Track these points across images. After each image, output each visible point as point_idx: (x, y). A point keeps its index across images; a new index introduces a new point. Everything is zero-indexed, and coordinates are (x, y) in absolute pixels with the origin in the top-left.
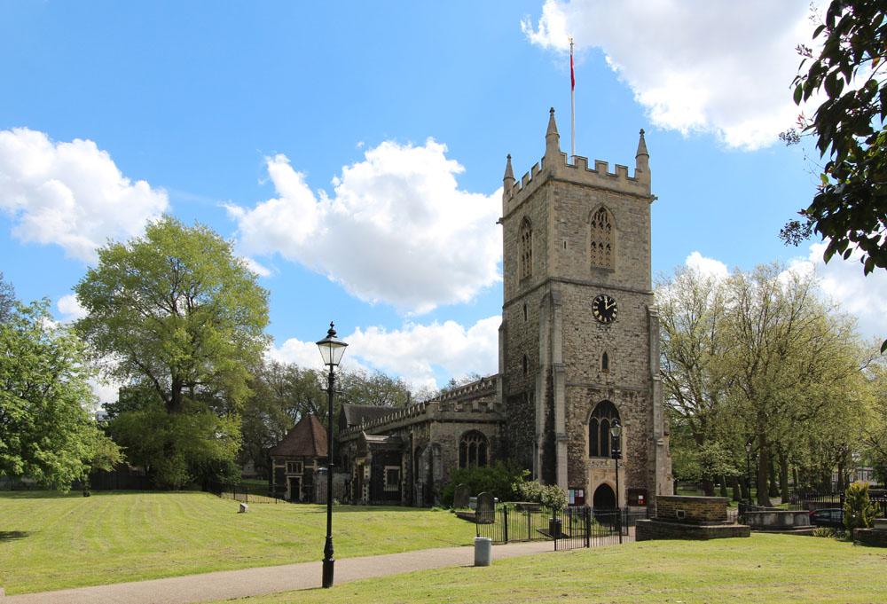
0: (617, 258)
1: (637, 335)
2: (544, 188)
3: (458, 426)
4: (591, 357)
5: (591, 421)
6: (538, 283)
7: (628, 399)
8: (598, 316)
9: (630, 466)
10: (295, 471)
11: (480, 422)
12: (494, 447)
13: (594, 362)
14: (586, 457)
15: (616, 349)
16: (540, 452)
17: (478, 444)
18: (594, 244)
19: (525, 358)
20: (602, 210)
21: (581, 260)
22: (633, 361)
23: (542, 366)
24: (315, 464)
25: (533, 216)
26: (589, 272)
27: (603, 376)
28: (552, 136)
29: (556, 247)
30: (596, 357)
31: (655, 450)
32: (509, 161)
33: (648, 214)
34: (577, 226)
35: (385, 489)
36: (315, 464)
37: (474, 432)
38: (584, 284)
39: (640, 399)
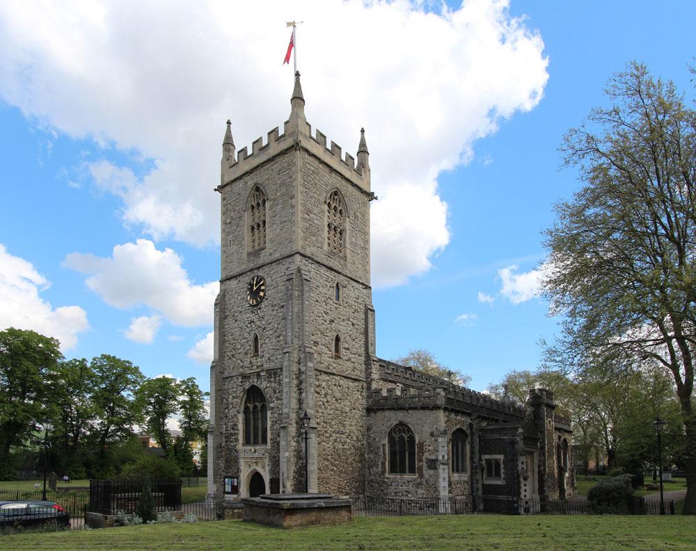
5: (245, 409)
14: (240, 446)
18: (253, 228)
27: (254, 360)
28: (298, 99)
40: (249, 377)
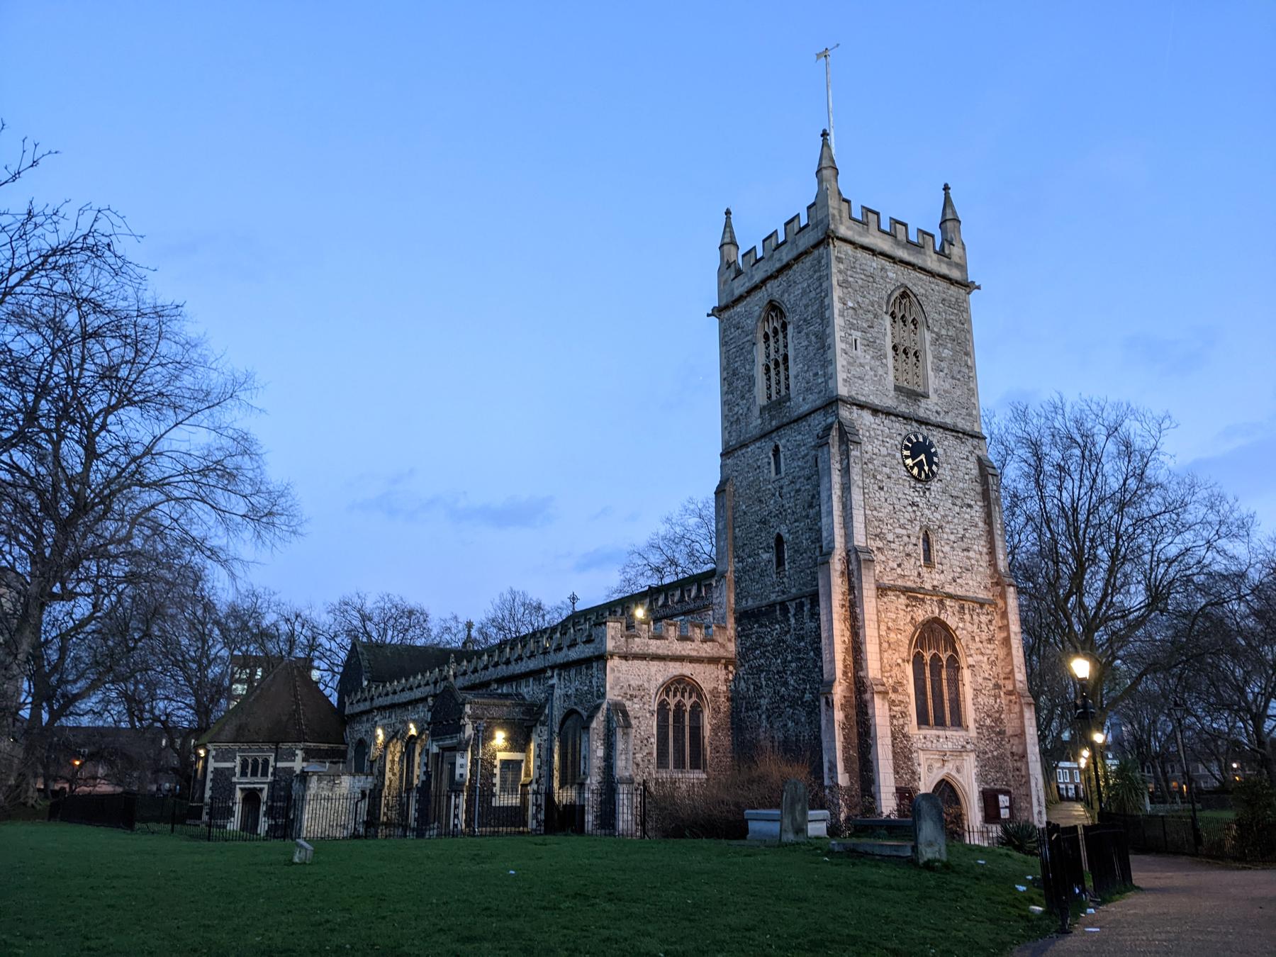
0: (931, 373)
1: (970, 506)
2: (816, 252)
3: (655, 666)
4: (906, 539)
6: (805, 408)
7: (967, 617)
8: (912, 468)
10: (254, 774)
11: (692, 660)
12: (716, 711)
13: (911, 546)
15: (940, 527)
16: (839, 715)
17: (688, 703)
18: (895, 348)
19: (779, 540)
20: (904, 295)
21: (880, 371)
22: (967, 550)
23: (830, 553)
24: (299, 758)
25: (788, 301)
26: (892, 393)
27: (924, 571)
29: (844, 346)
30: (913, 540)
31: (1021, 712)
32: (825, 144)
33: (967, 310)
34: (870, 316)
35: (496, 802)
36: (299, 758)
37: (680, 679)
38: (888, 413)
39: (984, 619)
40: (923, 600)
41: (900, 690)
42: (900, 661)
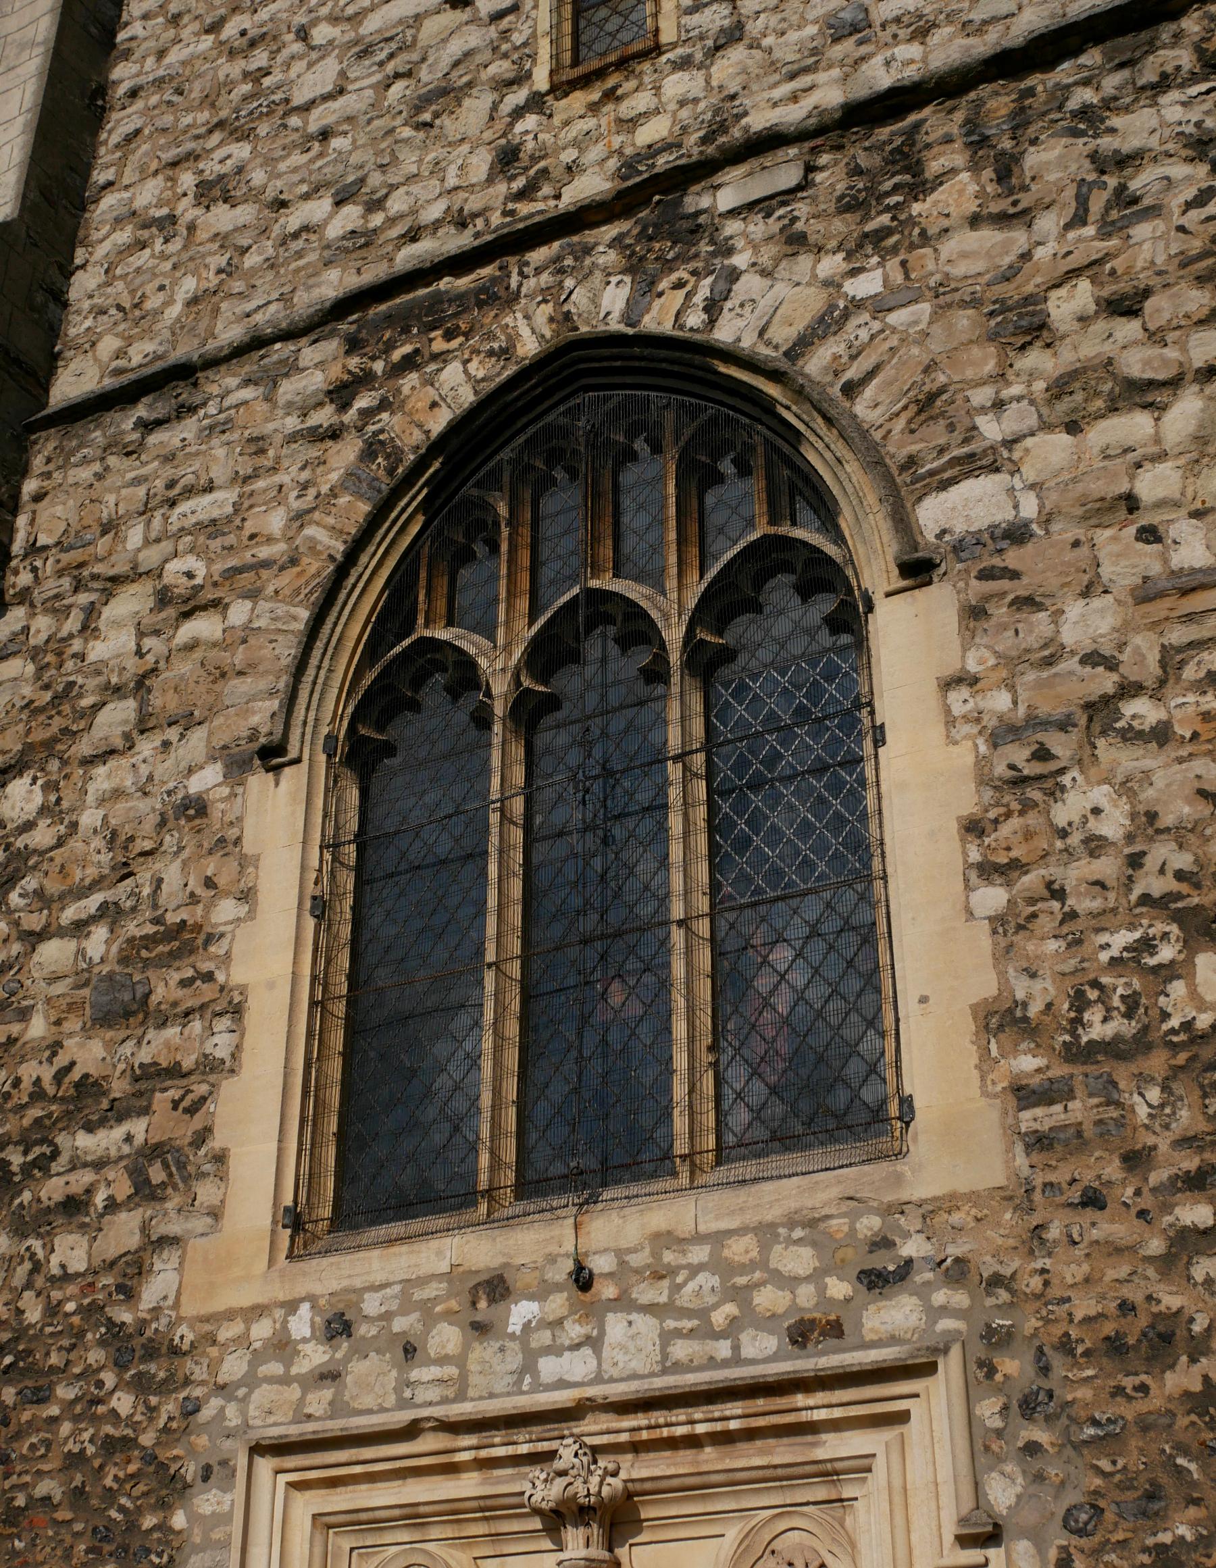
7: (959, 190)
9: (1088, 1277)
14: (233, 1259)
41: (165, 988)
42: (208, 779)
